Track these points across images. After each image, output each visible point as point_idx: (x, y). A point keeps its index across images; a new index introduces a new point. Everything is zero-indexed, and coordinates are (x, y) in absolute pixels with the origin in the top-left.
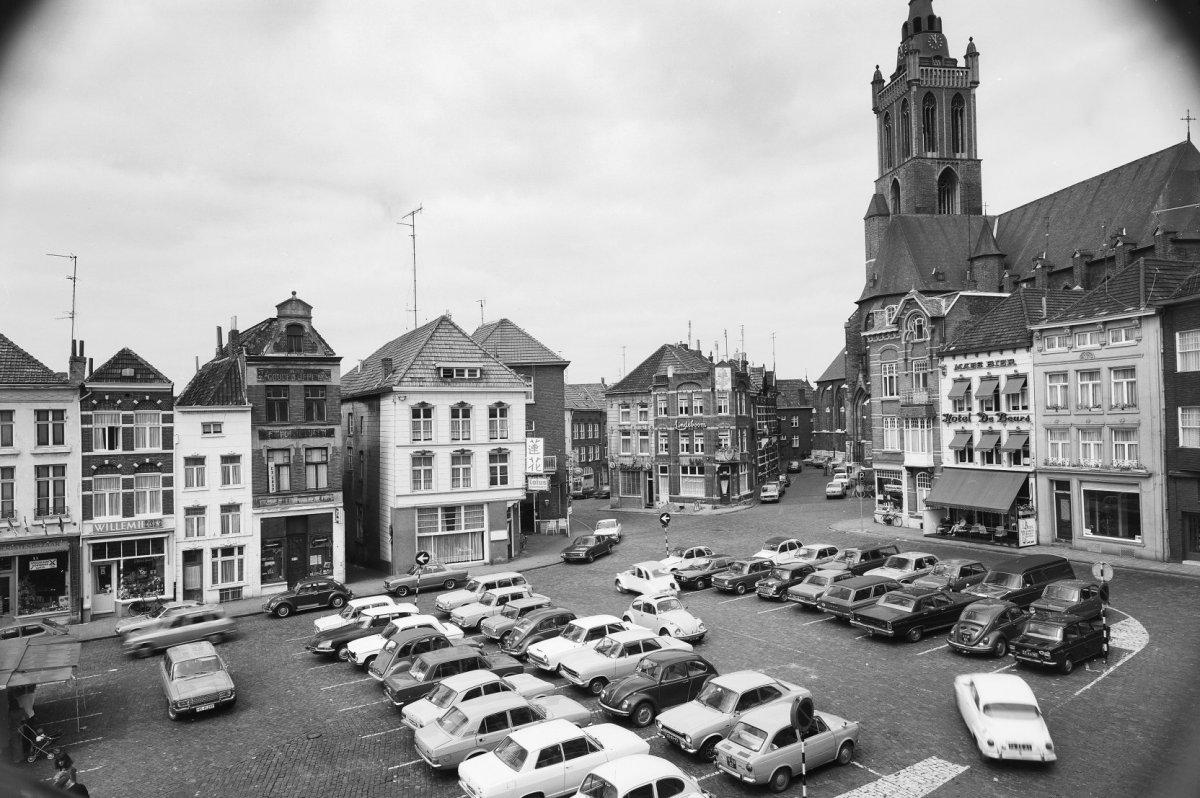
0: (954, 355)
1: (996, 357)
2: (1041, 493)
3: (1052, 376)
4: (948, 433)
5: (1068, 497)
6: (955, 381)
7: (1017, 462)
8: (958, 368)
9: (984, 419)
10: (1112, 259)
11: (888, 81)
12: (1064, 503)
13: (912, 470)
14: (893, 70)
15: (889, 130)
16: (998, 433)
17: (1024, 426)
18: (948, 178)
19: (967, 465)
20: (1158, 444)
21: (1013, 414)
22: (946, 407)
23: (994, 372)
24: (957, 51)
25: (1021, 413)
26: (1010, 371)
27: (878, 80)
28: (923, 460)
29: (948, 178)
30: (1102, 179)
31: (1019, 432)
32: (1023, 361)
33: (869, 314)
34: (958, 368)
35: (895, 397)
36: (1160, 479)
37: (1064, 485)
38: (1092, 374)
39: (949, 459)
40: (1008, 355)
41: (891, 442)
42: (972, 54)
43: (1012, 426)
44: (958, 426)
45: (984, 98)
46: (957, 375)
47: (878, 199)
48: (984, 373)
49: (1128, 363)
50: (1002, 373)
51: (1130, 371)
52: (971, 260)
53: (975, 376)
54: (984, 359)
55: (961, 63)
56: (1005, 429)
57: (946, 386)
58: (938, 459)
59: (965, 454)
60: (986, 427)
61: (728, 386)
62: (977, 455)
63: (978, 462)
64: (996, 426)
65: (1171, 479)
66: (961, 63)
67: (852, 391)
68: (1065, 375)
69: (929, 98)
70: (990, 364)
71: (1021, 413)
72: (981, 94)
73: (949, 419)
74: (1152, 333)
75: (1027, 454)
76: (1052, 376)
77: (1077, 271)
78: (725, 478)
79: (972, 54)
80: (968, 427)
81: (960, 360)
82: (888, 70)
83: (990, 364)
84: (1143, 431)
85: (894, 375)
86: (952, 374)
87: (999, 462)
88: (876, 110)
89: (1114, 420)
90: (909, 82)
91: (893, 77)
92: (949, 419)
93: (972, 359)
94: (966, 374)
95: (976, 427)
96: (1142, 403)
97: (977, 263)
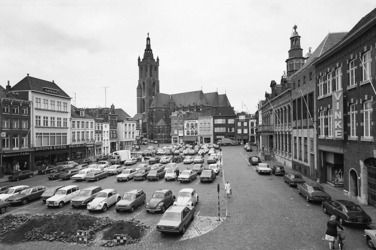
0: (187, 120)
1: (193, 121)
2: (199, 138)
3: (201, 124)
4: (186, 131)
5: (202, 139)
6: (187, 124)
7: (196, 135)
8: (187, 122)
9: (191, 129)
10: (194, 106)
11: (141, 60)
12: (202, 140)
13: (179, 137)
14: (143, 58)
15: (141, 70)
16: (193, 131)
17: (197, 130)
18: (154, 83)
19: (188, 135)
20: (213, 131)
21: (195, 128)
22: (185, 127)
23: (193, 123)
24: (155, 58)
25: (196, 128)
26: (195, 123)
27: (139, 59)
28: (182, 135)
29: (154, 83)
30: (189, 93)
31: (196, 131)
32: (197, 121)
33: (152, 111)
34: (187, 122)
35: (176, 126)
36: (213, 136)
37: (202, 137)
38: (205, 123)
39: (186, 135)
40: (195, 121)
41: (176, 132)
42: (158, 59)
43: (195, 130)
44: (187, 130)
46: (187, 123)
47: (139, 85)
48: (191, 123)
49: (210, 122)
50: (194, 123)
51: (209, 123)
52: (169, 103)
53: (190, 123)
54: (191, 121)
55: (156, 61)
56: (194, 131)
57: (185, 125)
58: (184, 135)
59: (188, 134)
60: (191, 130)
61: (141, 123)
62: (194, 134)
63: (194, 135)
64: (193, 130)
65: (214, 136)
66: (156, 61)
67: (149, 125)
68: (202, 123)
69: (151, 67)
70: (192, 122)
71: (196, 128)
73: (186, 129)
74: (212, 119)
75: (197, 133)
76: (201, 124)
77: (188, 108)
78: (140, 140)
80: (189, 130)
81: (188, 121)
82: (142, 58)
83: (192, 122)
84: (211, 130)
85: (176, 123)
86: (186, 123)
87: (193, 135)
89: (208, 129)
90: (148, 63)
92: (186, 129)
93: (189, 121)
94: (189, 123)
95: (190, 130)
96: (211, 127)
97: (171, 104)
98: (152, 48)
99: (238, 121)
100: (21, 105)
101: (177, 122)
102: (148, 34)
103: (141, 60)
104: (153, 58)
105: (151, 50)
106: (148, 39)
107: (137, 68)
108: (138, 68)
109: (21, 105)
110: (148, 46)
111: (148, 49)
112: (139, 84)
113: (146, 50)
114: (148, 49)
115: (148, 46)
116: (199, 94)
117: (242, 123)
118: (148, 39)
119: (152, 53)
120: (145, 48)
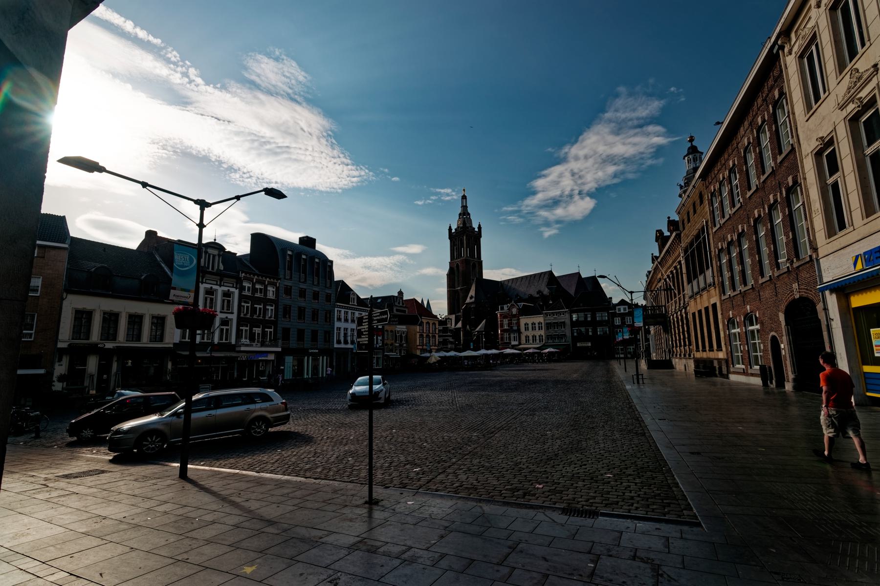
11: (453, 231)
14: (456, 227)
24: (475, 226)
27: (450, 229)
42: (480, 228)
45: (483, 241)
55: (476, 230)
66: (476, 230)
72: (482, 239)
79: (480, 228)
82: (454, 227)
88: (450, 238)
91: (456, 229)
98: (469, 210)
99: (615, 315)
100: (255, 281)
101: (508, 320)
102: (464, 190)
103: (453, 231)
104: (471, 226)
105: (469, 214)
106: (464, 197)
107: (447, 243)
108: (449, 241)
109: (255, 281)
110: (464, 207)
111: (465, 214)
112: (450, 267)
113: (460, 214)
114: (465, 214)
115: (464, 207)
116: (547, 276)
117: (623, 323)
118: (464, 197)
119: (470, 218)
120: (459, 210)
